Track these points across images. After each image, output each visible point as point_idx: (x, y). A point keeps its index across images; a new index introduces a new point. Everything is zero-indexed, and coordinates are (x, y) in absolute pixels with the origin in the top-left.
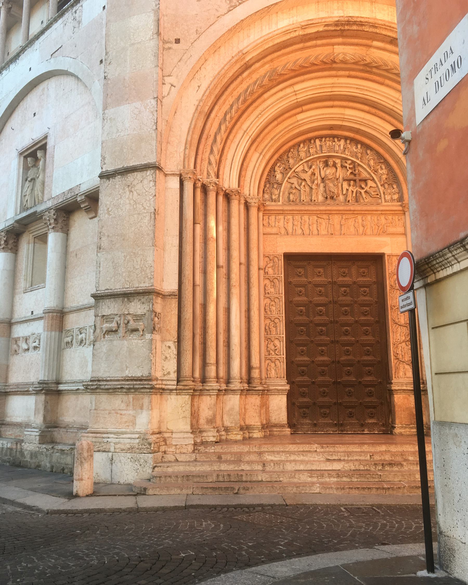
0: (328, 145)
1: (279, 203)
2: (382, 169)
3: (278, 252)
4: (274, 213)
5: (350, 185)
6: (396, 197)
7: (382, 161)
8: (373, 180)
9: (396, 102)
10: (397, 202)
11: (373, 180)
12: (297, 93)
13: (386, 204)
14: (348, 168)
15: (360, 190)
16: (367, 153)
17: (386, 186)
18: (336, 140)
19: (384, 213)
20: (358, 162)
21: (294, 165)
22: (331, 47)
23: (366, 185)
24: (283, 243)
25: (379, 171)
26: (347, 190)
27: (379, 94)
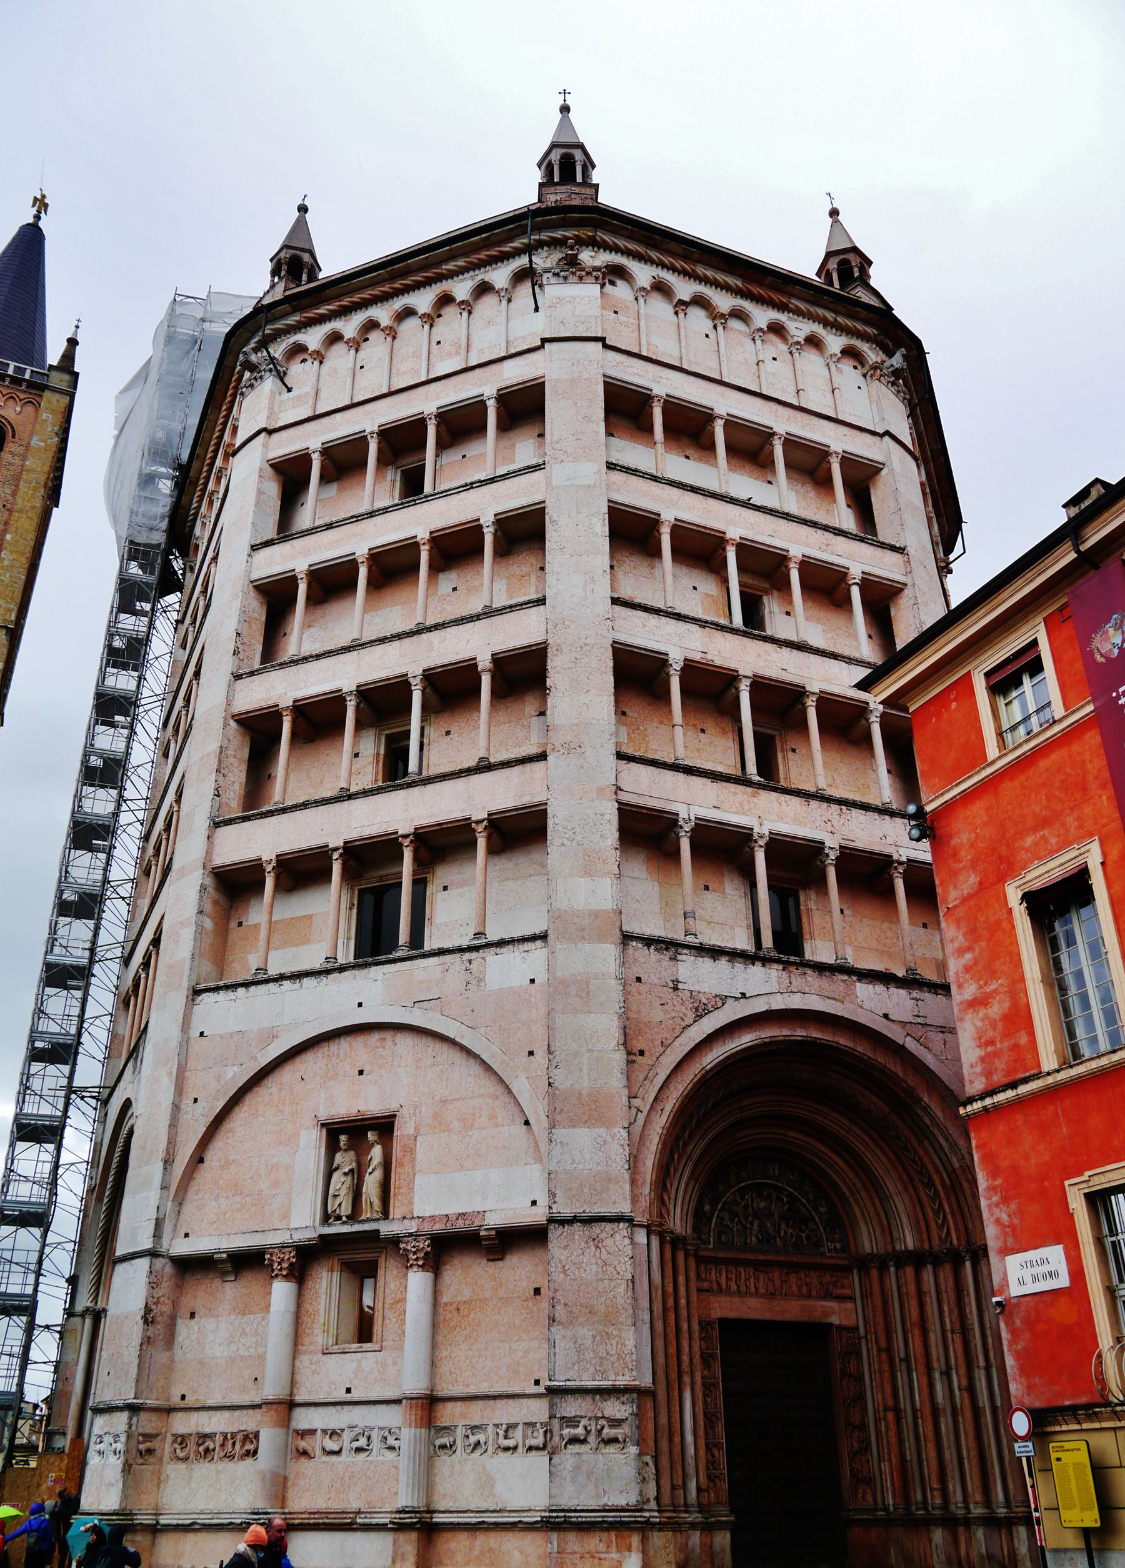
5: (788, 1226)
23: (807, 1227)
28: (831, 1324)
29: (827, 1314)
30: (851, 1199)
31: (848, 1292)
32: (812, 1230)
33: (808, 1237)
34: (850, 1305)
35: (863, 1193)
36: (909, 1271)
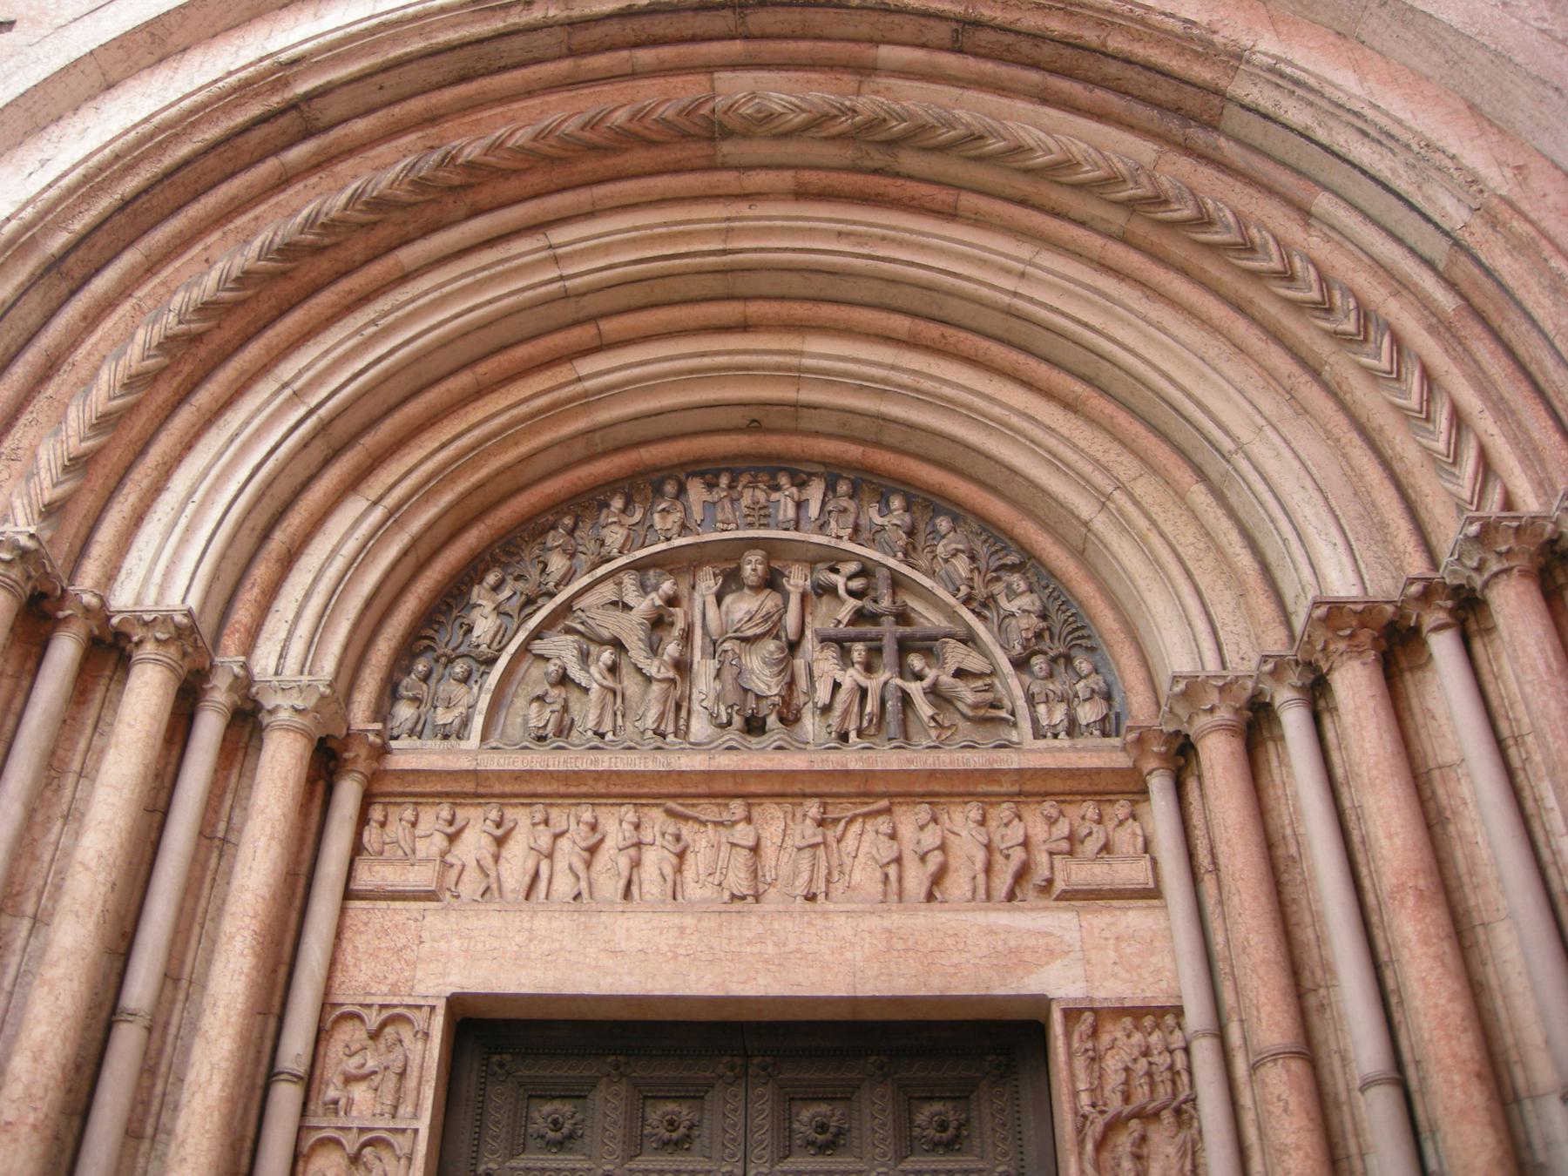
0: (746, 500)
1: (464, 745)
2: (1011, 594)
3: (421, 989)
4: (428, 789)
6: (1088, 713)
7: (1013, 559)
8: (970, 639)
9: (1022, 275)
10: (1105, 734)
11: (970, 639)
12: (560, 251)
13: (1041, 743)
14: (841, 591)
15: (899, 681)
16: (934, 531)
17: (1038, 663)
18: (784, 480)
19: (1030, 788)
20: (892, 562)
21: (567, 578)
22: (703, 79)
24: (456, 943)
25: (1003, 602)
26: (837, 686)
27: (943, 252)
28: (1042, 1003)
29: (1017, 959)
30: (1100, 523)
31: (1133, 873)
32: (960, 673)
33: (934, 692)
34: (1136, 918)
35: (1145, 488)
36: (1354, 684)
